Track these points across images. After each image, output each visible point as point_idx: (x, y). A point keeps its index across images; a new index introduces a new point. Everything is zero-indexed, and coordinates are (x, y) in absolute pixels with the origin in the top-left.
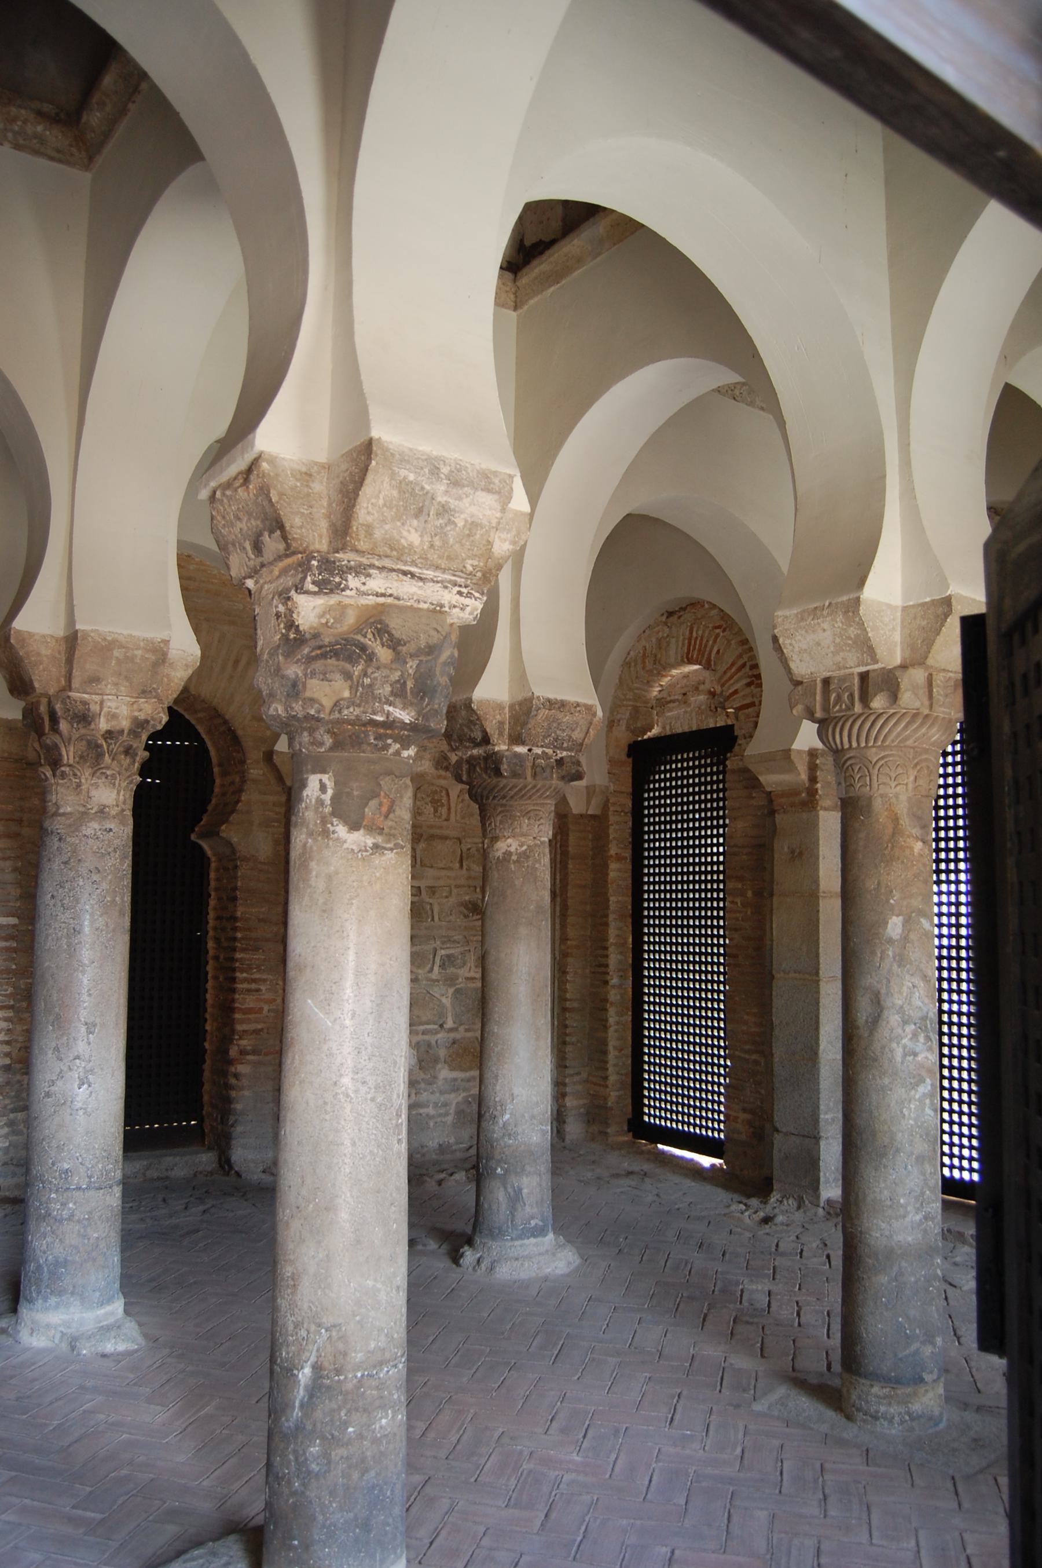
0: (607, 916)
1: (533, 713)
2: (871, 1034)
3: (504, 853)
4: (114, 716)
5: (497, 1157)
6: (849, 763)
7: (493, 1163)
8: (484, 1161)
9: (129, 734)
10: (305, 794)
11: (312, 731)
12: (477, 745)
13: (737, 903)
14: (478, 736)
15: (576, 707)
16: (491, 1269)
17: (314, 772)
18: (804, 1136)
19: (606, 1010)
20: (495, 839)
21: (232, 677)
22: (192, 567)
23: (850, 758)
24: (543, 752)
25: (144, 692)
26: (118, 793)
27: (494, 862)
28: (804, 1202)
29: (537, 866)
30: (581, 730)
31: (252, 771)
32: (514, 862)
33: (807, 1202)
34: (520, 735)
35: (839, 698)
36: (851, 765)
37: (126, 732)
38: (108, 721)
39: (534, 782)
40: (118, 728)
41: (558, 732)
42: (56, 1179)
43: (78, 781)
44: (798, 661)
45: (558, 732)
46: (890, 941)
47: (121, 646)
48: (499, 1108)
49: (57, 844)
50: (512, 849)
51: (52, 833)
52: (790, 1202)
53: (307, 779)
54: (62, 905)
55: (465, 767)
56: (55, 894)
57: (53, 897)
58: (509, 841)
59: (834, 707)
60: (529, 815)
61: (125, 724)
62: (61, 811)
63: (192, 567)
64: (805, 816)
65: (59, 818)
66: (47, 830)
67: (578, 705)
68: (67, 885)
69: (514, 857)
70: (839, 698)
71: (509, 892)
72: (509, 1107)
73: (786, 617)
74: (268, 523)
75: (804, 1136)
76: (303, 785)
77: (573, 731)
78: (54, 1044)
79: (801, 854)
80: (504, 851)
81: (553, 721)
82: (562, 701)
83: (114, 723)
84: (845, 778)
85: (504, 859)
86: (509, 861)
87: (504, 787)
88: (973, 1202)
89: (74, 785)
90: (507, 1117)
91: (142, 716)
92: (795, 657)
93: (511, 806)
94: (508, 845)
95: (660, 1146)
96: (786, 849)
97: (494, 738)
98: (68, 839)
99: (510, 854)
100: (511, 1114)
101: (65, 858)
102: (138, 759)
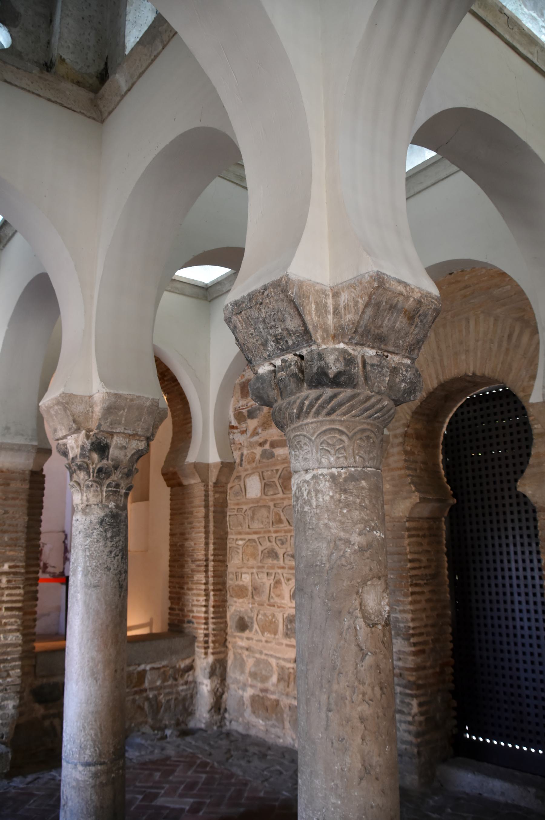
4: (72, 448)
9: (80, 457)
15: (263, 293)
21: (508, 350)
22: (466, 278)
24: (284, 361)
25: (70, 429)
26: (82, 495)
29: (306, 509)
30: (290, 314)
31: (536, 426)
37: (78, 456)
38: (72, 451)
39: (282, 402)
40: (75, 455)
41: (271, 331)
45: (271, 331)
47: (51, 407)
61: (77, 451)
63: (466, 278)
67: (265, 288)
77: (283, 321)
81: (256, 323)
82: (249, 295)
83: (73, 452)
91: (80, 443)
102: (91, 471)
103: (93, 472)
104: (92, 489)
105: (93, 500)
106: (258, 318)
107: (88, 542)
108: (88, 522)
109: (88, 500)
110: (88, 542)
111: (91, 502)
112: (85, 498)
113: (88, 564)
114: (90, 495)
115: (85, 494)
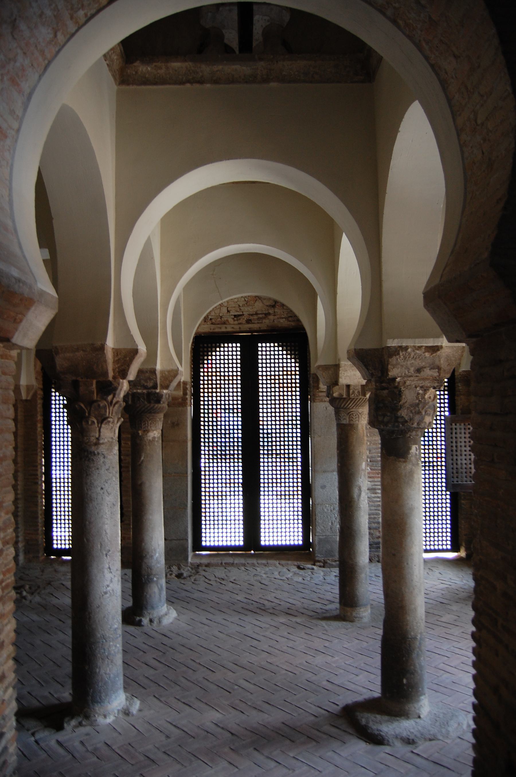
0: (37, 450)
2: (358, 500)
5: (154, 573)
6: (352, 413)
7: (152, 577)
8: (146, 577)
10: (411, 452)
11: (417, 431)
12: (145, 387)
13: (128, 444)
14: (150, 384)
16: (160, 622)
17: (414, 444)
18: (179, 540)
19: (37, 497)
20: (148, 431)
23: (352, 411)
27: (147, 442)
28: (181, 566)
33: (182, 566)
35: (353, 392)
36: (352, 414)
42: (112, 635)
43: (112, 425)
44: (344, 379)
46: (363, 470)
48: (154, 552)
49: (102, 460)
50: (156, 436)
51: (98, 454)
52: (174, 567)
53: (411, 447)
54: (108, 492)
55: (130, 397)
56: (103, 487)
57: (102, 489)
58: (155, 432)
59: (352, 394)
62: (101, 441)
64: (180, 409)
65: (102, 446)
66: (94, 452)
68: (109, 482)
69: (156, 439)
70: (353, 392)
72: (158, 550)
73: (346, 365)
74: (432, 366)
75: (179, 540)
76: (410, 448)
78: (107, 566)
79: (178, 425)
84: (349, 417)
85: (153, 440)
87: (157, 408)
88: (69, 558)
89: (110, 427)
90: (157, 555)
92: (343, 378)
95: (197, 552)
96: (169, 422)
98: (109, 457)
100: (159, 553)
101: (107, 467)
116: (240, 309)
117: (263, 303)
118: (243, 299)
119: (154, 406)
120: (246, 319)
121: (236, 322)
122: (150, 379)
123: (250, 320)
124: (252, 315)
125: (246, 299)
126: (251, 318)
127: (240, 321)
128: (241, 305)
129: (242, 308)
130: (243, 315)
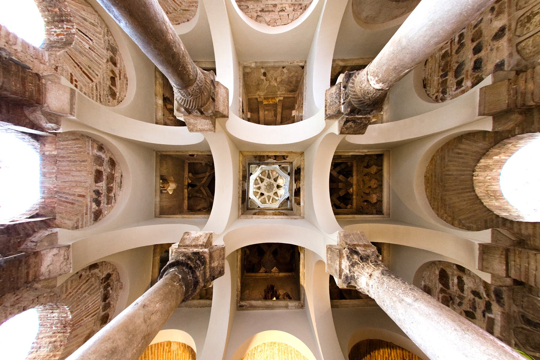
1: (328, 116)
3: (378, 83)
32: (378, 77)
34: (338, 113)
50: (374, 82)
60: (369, 80)
69: (377, 79)
71: (391, 68)
80: (378, 85)
85: (381, 82)
86: (379, 79)
93: (362, 95)
94: (376, 85)
97: (345, 119)
99: (377, 81)
103: (359, 261)
104: (365, 268)
105: (370, 271)
106: (330, 104)
107: (385, 285)
108: (377, 279)
109: (368, 273)
110: (385, 285)
111: (370, 272)
112: (366, 274)
113: (397, 294)
114: (367, 270)
115: (365, 273)
116: (280, 16)
117: (264, 19)
118: (278, 24)
119: (358, 107)
120: (277, 8)
121: (284, 5)
122: (347, 128)
123: (274, 6)
124: (272, 11)
125: (275, 24)
126: (273, 9)
127: (282, 6)
128: (279, 20)
129: (279, 17)
130: (278, 12)
